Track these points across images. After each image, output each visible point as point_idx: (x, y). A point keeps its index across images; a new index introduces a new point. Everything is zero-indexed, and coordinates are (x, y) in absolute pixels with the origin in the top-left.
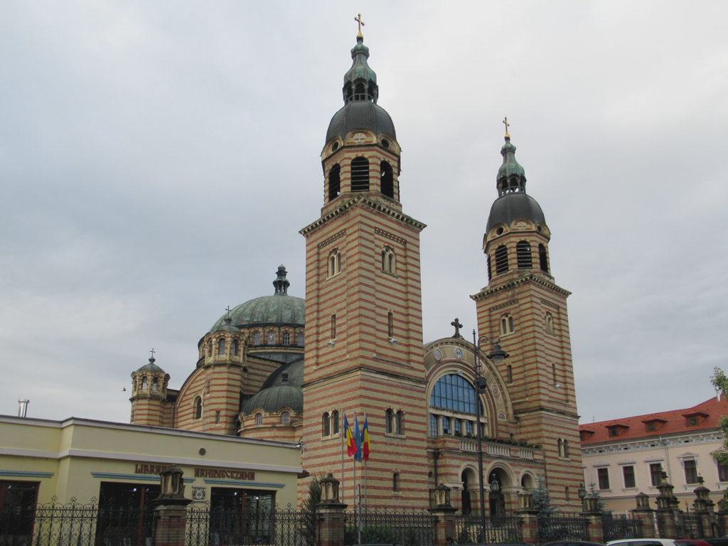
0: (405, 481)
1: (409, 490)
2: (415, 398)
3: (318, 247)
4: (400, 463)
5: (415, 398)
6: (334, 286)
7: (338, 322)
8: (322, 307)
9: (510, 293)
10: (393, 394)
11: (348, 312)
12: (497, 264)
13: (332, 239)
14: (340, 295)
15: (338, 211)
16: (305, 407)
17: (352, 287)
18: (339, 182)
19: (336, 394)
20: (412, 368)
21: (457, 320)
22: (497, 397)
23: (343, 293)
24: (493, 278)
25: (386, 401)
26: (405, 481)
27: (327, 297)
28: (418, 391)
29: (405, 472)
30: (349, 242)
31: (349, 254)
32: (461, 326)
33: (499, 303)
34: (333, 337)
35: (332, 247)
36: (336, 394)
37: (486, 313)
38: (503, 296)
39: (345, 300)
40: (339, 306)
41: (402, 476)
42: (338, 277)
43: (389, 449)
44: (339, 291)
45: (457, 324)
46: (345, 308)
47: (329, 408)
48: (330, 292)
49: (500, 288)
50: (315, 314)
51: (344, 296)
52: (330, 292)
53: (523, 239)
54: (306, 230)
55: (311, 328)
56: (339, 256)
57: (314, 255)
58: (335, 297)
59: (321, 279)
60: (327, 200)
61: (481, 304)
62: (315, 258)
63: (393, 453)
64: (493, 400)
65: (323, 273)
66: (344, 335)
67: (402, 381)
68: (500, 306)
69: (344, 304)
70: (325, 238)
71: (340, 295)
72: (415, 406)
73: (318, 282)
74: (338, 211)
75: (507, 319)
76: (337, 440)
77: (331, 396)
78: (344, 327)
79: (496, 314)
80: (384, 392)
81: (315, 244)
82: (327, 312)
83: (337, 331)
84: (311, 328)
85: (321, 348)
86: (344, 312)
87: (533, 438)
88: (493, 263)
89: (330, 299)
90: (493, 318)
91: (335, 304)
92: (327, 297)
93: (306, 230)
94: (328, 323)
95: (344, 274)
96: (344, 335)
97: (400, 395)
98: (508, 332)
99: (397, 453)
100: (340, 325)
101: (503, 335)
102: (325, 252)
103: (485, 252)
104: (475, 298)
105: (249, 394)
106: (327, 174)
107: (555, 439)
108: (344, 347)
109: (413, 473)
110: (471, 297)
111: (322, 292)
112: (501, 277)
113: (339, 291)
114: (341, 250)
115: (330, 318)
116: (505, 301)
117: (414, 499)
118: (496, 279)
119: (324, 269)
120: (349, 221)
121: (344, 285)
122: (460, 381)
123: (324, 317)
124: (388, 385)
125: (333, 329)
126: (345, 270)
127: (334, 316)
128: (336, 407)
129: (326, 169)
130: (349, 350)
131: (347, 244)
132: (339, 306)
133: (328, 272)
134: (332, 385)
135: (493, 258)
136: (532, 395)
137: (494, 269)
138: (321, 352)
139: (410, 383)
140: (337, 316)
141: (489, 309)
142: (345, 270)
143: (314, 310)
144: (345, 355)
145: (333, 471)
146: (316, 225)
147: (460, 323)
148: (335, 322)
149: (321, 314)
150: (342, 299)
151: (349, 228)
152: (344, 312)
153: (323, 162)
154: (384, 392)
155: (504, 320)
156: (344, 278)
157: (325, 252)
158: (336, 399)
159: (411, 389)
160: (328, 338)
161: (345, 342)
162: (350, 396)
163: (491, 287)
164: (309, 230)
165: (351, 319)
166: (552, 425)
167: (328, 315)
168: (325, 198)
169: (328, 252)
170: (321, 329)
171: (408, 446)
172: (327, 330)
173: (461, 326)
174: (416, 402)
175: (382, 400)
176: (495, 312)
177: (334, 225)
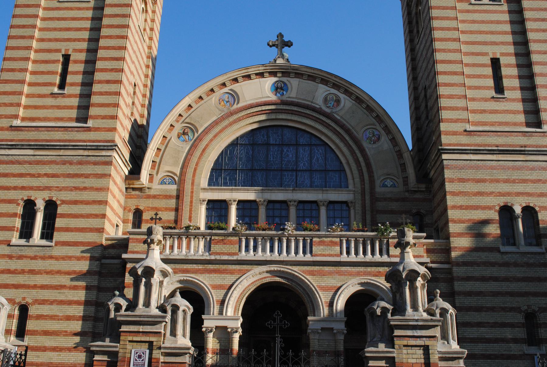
0: (39, 317)
1: (46, 333)
2: (87, 176)
4: (35, 287)
5: (87, 176)
10: (39, 175)
20: (89, 129)
21: (281, 35)
25: (23, 188)
26: (39, 317)
28: (95, 163)
32: (289, 44)
41: (32, 311)
43: (14, 265)
63: (23, 272)
67: (62, 152)
72: (85, 189)
80: (21, 175)
97: (54, 176)
99: (32, 272)
107: (489, 208)
109: (61, 302)
117: (54, 349)
124: (30, 163)
139: (81, 152)
147: (286, 39)
154: (21, 175)
159: (80, 163)
166: (478, 181)
171: (57, 258)
173: (289, 44)
174: (88, 183)
175: (15, 188)
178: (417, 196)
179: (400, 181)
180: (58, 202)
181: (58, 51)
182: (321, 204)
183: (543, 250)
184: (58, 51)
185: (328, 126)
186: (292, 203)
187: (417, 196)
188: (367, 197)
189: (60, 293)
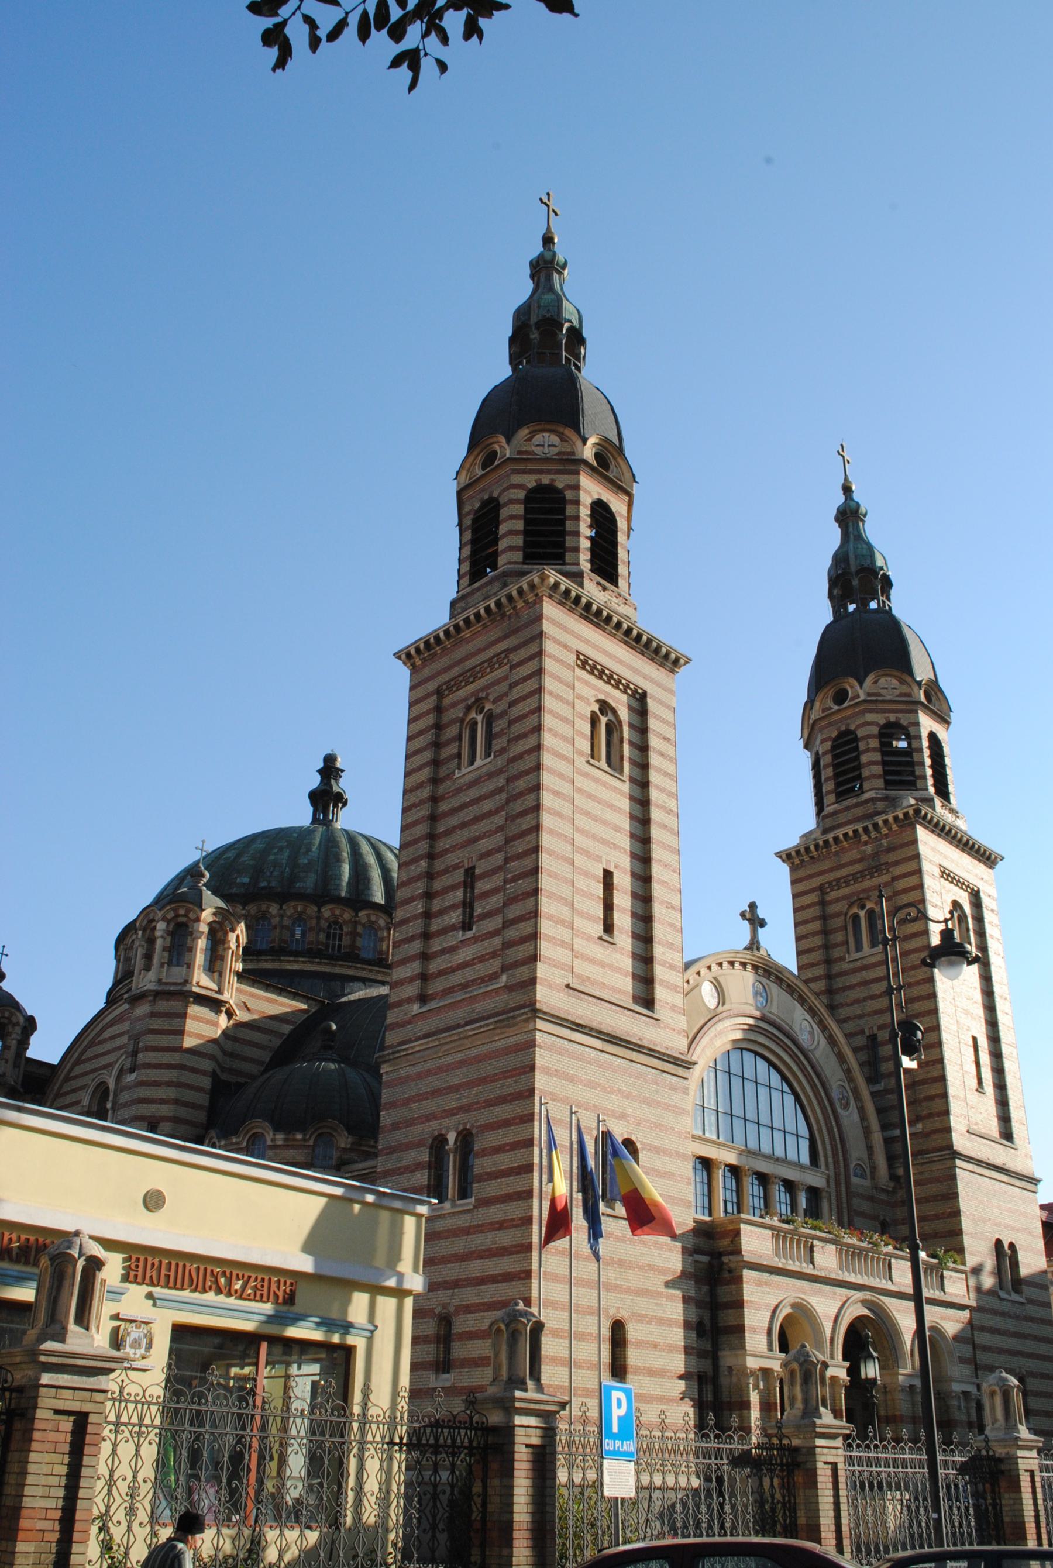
3: (439, 693)
4: (628, 1291)
6: (473, 793)
7: (481, 886)
8: (443, 844)
11: (507, 860)
12: (836, 775)
13: (473, 675)
14: (490, 814)
15: (493, 606)
16: (386, 1118)
17: (521, 794)
18: (495, 541)
19: (470, 1084)
21: (753, 906)
22: (846, 1107)
23: (497, 811)
24: (828, 810)
27: (454, 821)
29: (641, 1318)
30: (517, 683)
31: (516, 711)
32: (762, 923)
33: (844, 872)
34: (466, 926)
35: (472, 694)
36: (470, 1084)
37: (813, 898)
39: (500, 829)
40: (485, 844)
42: (484, 770)
44: (487, 806)
45: (754, 919)
46: (499, 850)
47: (450, 1122)
48: (464, 806)
49: (846, 835)
50: (423, 864)
51: (499, 820)
52: (464, 806)
54: (413, 652)
55: (412, 899)
56: (490, 719)
57: (428, 713)
58: (477, 819)
59: (443, 772)
60: (466, 581)
61: (802, 873)
62: (430, 720)
64: (837, 1117)
65: (450, 759)
66: (496, 922)
68: (846, 881)
69: (499, 839)
70: (456, 671)
71: (490, 814)
73: (435, 781)
74: (493, 606)
75: (862, 913)
76: (468, 1217)
77: (456, 1088)
78: (496, 900)
79: (838, 900)
81: (431, 686)
82: (452, 859)
83: (478, 911)
84: (412, 899)
85: (435, 955)
86: (498, 859)
88: (827, 773)
89: (463, 825)
90: (833, 909)
91: (475, 840)
92: (454, 821)
93: (413, 652)
94: (453, 888)
95: (500, 762)
96: (496, 922)
100: (486, 894)
101: (855, 956)
102: (454, 705)
103: (807, 746)
104: (787, 856)
105: (233, 1079)
106: (468, 521)
108: (493, 955)
110: (778, 855)
111: (444, 807)
112: (847, 809)
113: (487, 806)
114: (494, 702)
115: (459, 876)
116: (858, 867)
118: (835, 813)
119: (452, 749)
120: (517, 631)
121: (500, 790)
122: (762, 1065)
123: (446, 871)
125: (468, 905)
126: (503, 750)
127: (470, 872)
128: (464, 1119)
129: (467, 508)
130: (509, 961)
131: (512, 686)
132: (485, 844)
133: (459, 755)
134: (458, 1057)
135: (826, 760)
136: (930, 1116)
137: (828, 786)
138: (434, 967)
140: (477, 871)
141: (821, 888)
142: (503, 750)
143: (421, 852)
144: (495, 976)
145: (452, 1309)
146: (437, 638)
147: (761, 913)
148: (473, 888)
149: (439, 865)
150: (493, 827)
151: (516, 648)
152: (498, 859)
153: (460, 493)
155: (856, 918)
156: (500, 772)
157: (454, 705)
158: (467, 1097)
160: (453, 928)
161: (497, 941)
162: (506, 1091)
163: (825, 832)
164: (418, 650)
165: (514, 879)
167: (456, 867)
168: (460, 577)
169: (462, 705)
170: (437, 905)
172: (453, 907)
173: (762, 923)
176: (833, 895)
177: (480, 642)
178: (883, 1197)
179: (868, 1170)
180: (639, 1146)
181: (598, 859)
182: (801, 1187)
183: (1023, 1300)
184: (598, 859)
185: (803, 1069)
186: (777, 1180)
187: (883, 1197)
188: (843, 1189)
189: (657, 1304)
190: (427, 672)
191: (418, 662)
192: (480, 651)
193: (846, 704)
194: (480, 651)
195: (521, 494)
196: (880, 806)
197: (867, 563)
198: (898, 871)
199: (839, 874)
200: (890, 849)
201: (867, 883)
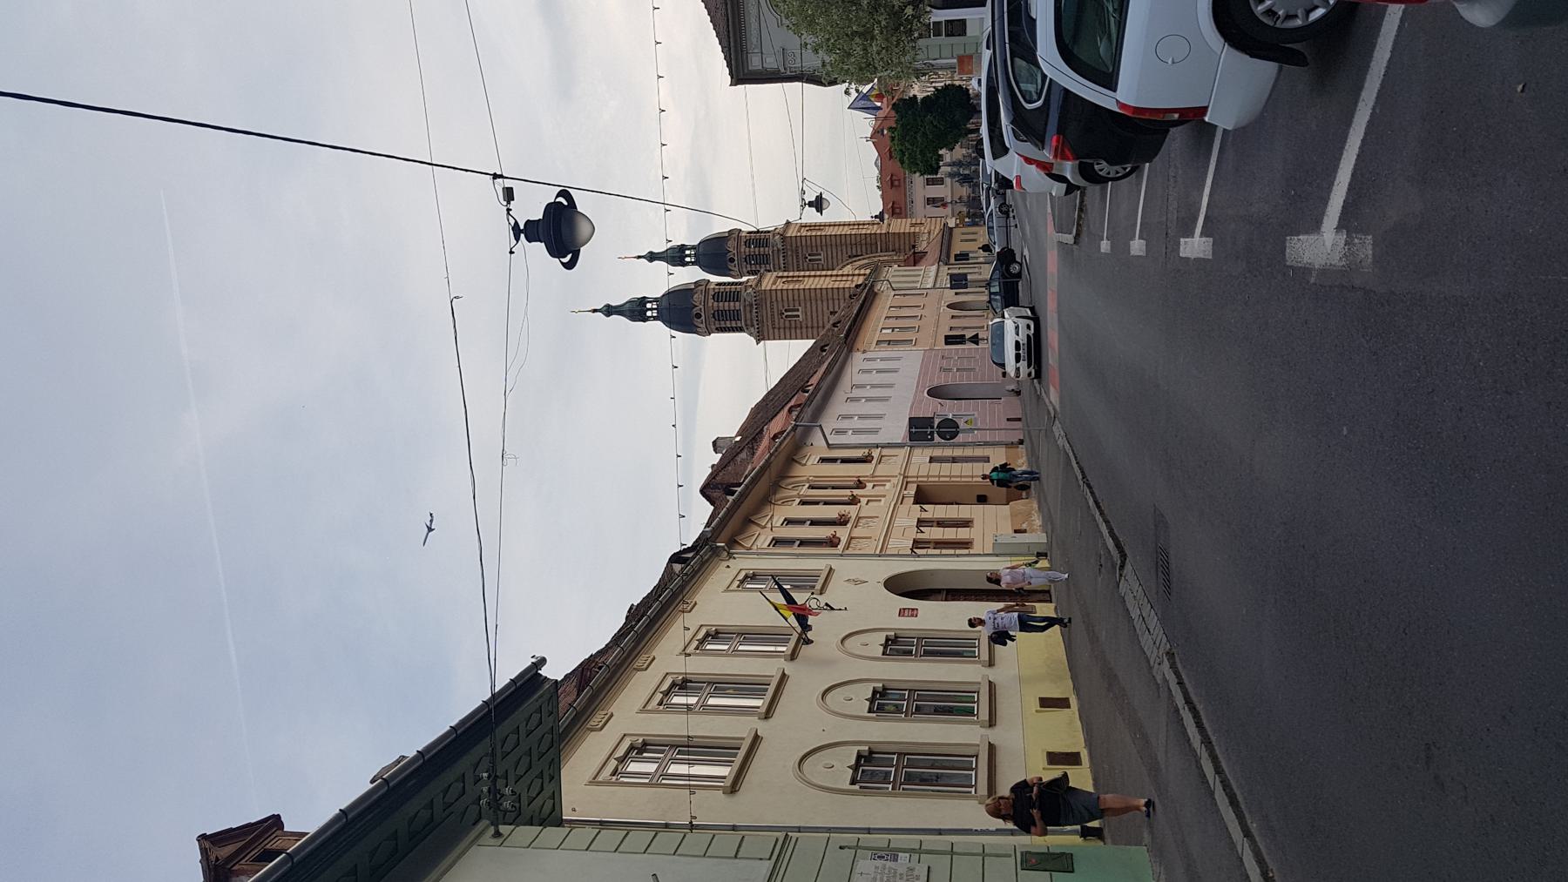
6: (809, 314)
9: (789, 253)
13: (773, 315)
38: (790, 258)
40: (825, 309)
44: (814, 308)
53: (743, 243)
56: (786, 311)
81: (771, 331)
87: (909, 240)
95: (803, 304)
98: (821, 257)
111: (809, 325)
113: (814, 308)
132: (825, 309)
151: (771, 299)
155: (810, 260)
190: (766, 334)
191: (761, 337)
192: (767, 313)
193: (736, 259)
194: (767, 313)
195: (716, 304)
196: (775, 248)
197: (677, 250)
198: (799, 244)
199: (795, 265)
200: (791, 246)
201: (800, 255)
